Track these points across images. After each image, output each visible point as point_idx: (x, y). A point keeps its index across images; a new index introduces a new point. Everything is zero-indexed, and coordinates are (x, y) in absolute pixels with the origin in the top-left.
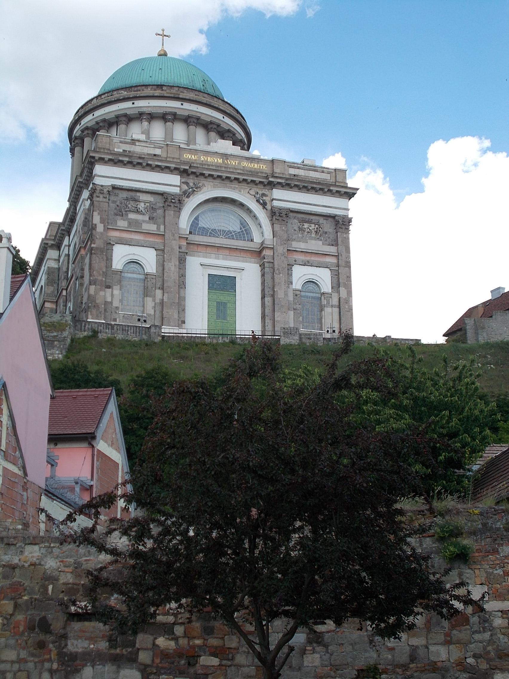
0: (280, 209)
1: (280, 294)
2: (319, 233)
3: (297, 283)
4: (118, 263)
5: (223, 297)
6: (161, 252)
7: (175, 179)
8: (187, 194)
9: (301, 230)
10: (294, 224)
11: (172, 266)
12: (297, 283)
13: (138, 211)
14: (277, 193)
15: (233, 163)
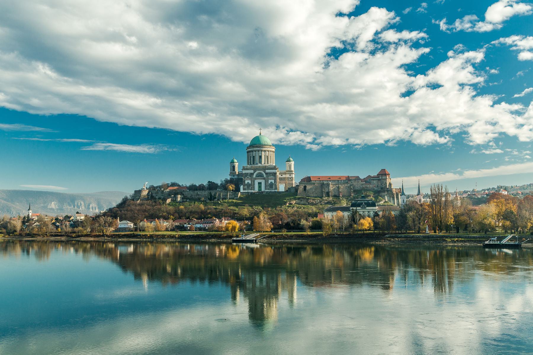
0: (267, 173)
1: (267, 184)
2: (273, 175)
3: (269, 183)
4: (246, 183)
5: (260, 185)
6: (251, 181)
7: (253, 171)
8: (254, 172)
9: (270, 175)
10: (269, 174)
11: (253, 183)
12: (269, 183)
13: (248, 176)
14: (266, 171)
15: (260, 167)
